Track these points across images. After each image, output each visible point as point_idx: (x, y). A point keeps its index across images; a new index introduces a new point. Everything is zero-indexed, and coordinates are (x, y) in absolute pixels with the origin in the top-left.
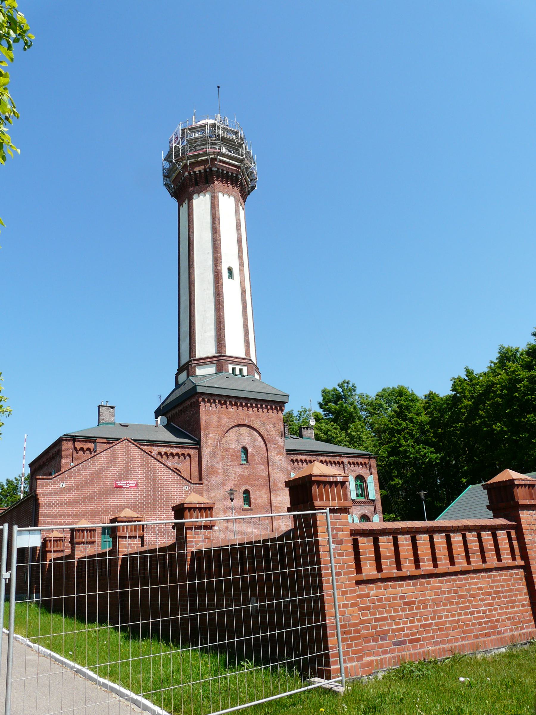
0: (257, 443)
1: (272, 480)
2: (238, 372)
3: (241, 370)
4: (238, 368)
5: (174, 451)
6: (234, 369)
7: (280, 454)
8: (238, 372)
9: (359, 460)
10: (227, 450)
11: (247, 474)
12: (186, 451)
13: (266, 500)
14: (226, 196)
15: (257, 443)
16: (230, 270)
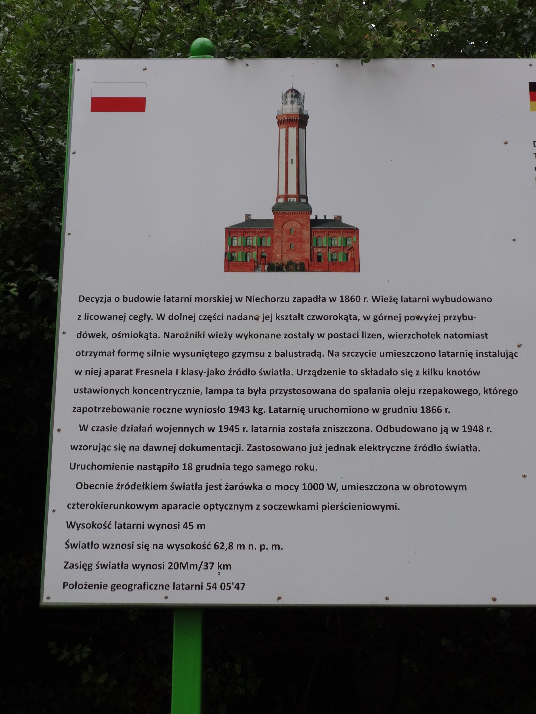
0: (297, 226)
1: (303, 239)
2: (292, 201)
3: (293, 200)
4: (292, 199)
5: (264, 231)
6: (290, 200)
7: (308, 230)
8: (292, 201)
9: (349, 231)
10: (284, 229)
11: (292, 237)
12: (268, 230)
13: (300, 247)
14: (293, 128)
15: (297, 226)
16: (292, 160)
